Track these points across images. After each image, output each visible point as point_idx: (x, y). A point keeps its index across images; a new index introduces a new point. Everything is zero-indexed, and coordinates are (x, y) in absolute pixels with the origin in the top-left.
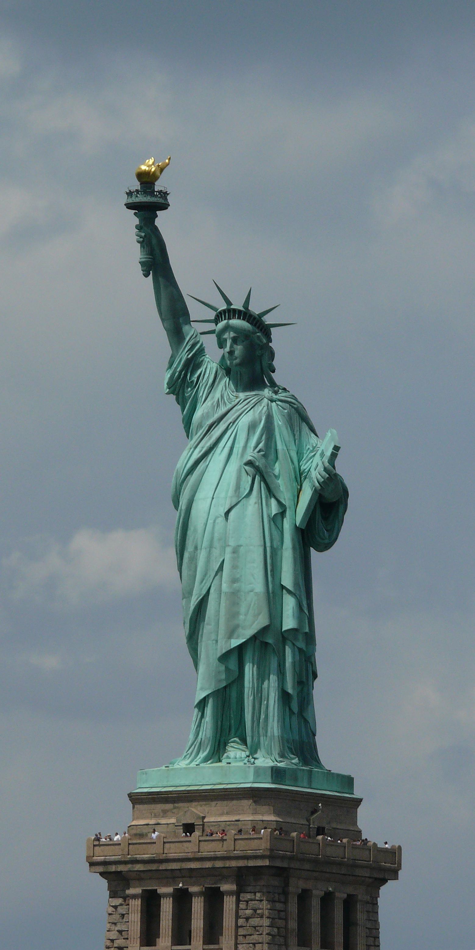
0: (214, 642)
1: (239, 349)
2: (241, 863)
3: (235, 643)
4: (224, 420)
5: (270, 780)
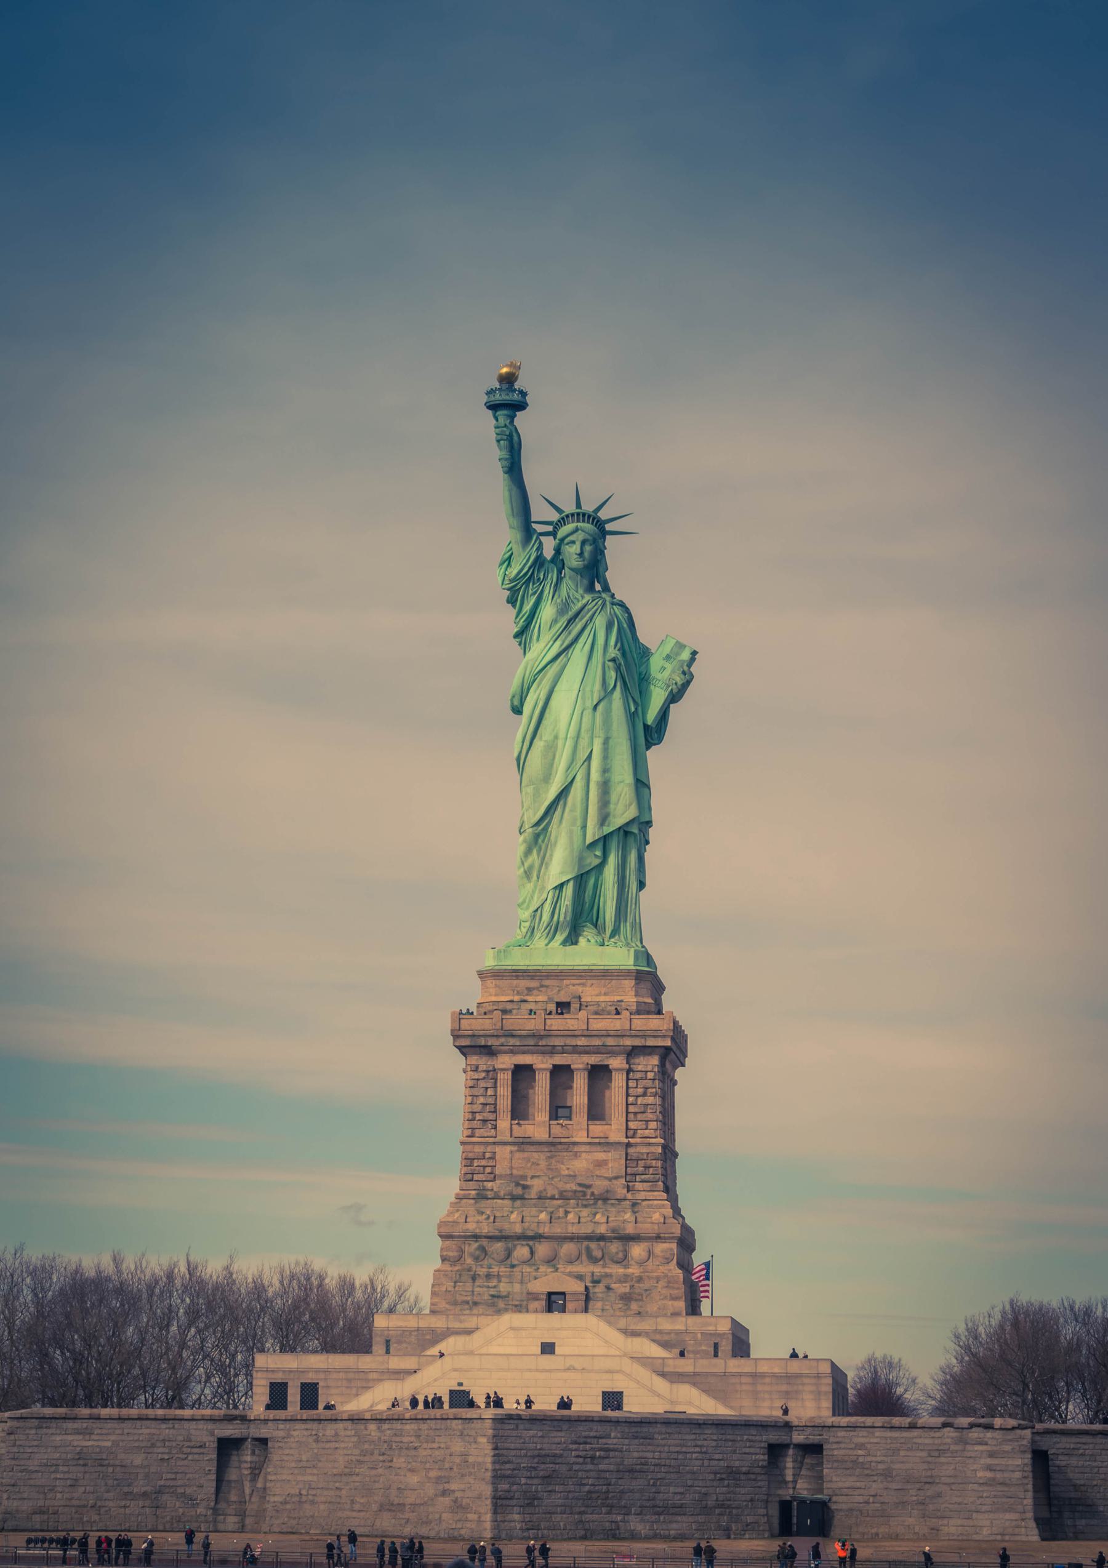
0: (579, 828)
2: (638, 1042)
3: (607, 830)
4: (580, 616)
5: (646, 965)
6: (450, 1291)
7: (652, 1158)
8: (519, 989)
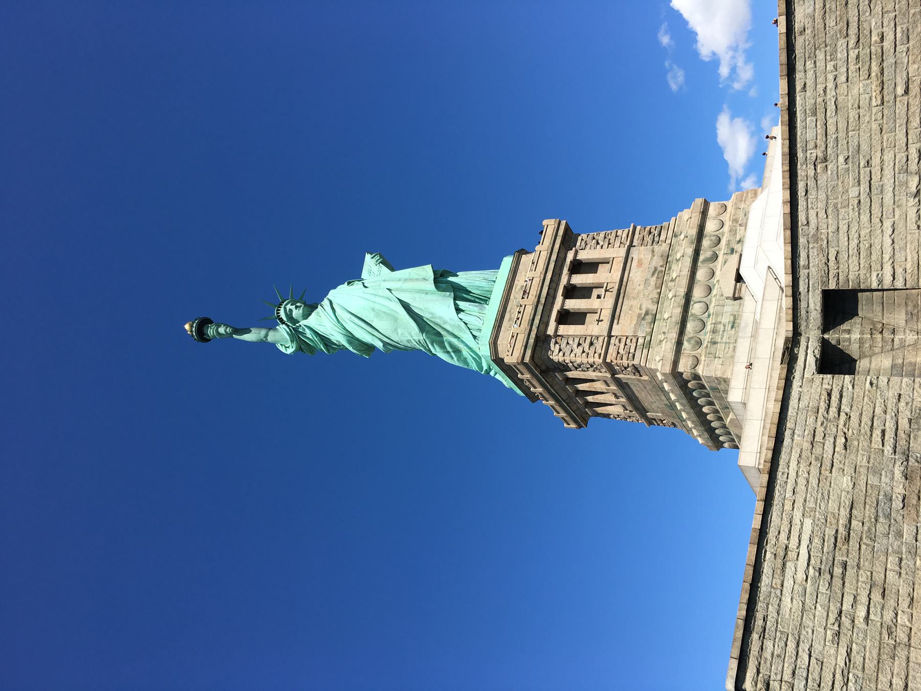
1: (298, 304)
6: (723, 362)
7: (643, 231)
8: (508, 327)
